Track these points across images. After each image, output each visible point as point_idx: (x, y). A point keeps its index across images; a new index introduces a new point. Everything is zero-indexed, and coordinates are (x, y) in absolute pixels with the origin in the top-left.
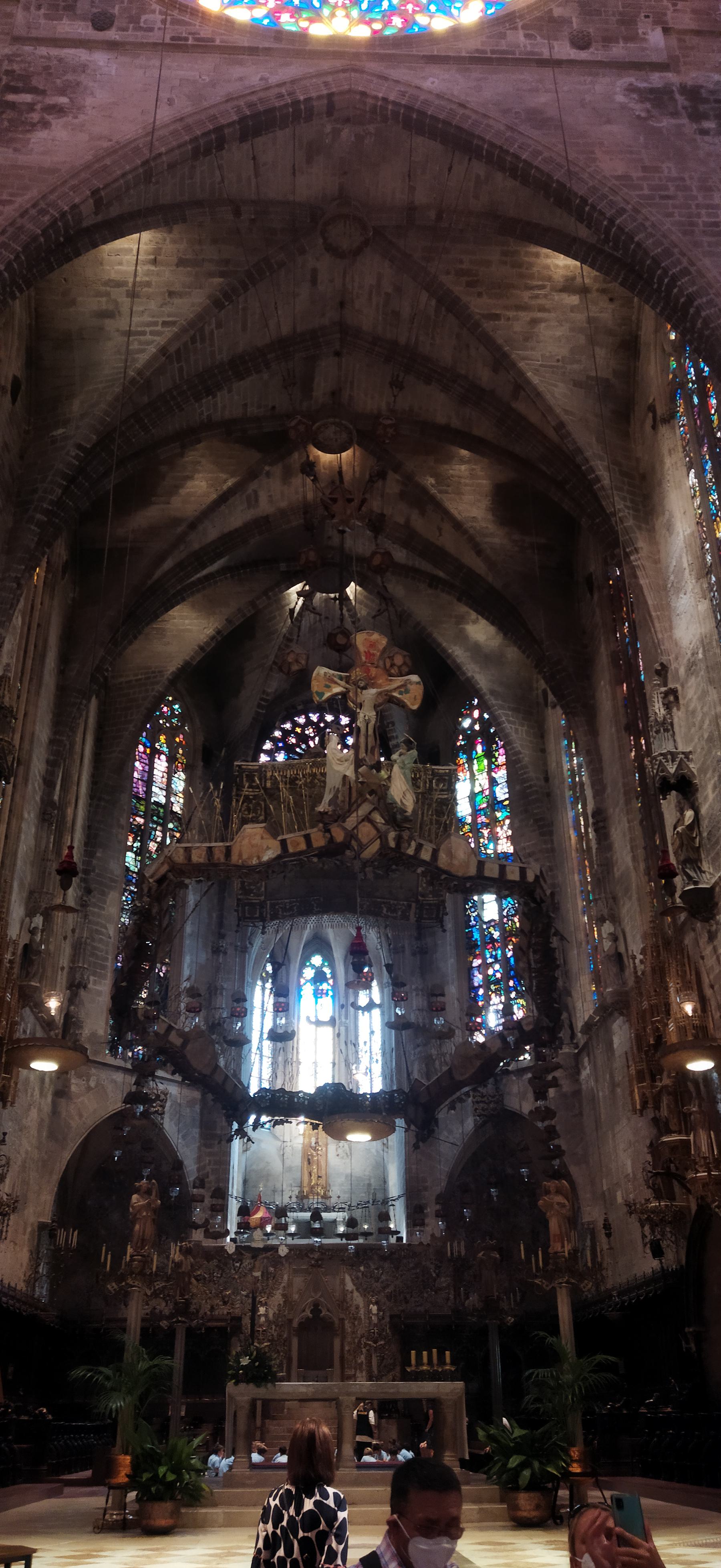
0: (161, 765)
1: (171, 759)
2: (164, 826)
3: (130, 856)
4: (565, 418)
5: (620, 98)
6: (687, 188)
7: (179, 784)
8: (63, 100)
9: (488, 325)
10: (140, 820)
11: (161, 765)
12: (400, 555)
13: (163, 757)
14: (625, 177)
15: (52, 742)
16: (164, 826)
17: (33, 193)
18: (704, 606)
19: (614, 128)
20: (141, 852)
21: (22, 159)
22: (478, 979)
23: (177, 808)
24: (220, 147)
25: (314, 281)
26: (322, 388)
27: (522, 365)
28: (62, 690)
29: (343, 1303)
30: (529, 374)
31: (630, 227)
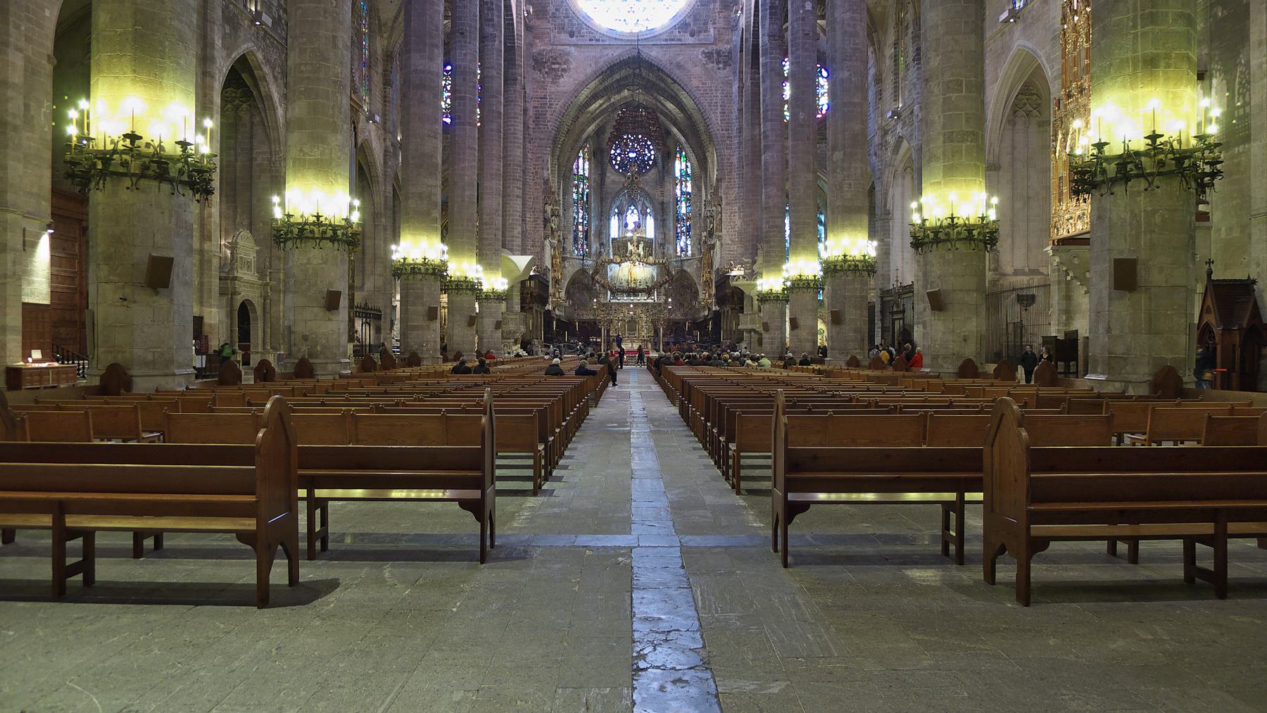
1: (584, 158)
2: (583, 182)
3: (574, 195)
4: (693, 111)
6: (712, 90)
7: (587, 166)
10: (576, 182)
11: (581, 161)
13: (581, 158)
16: (583, 182)
19: (697, 68)
20: (577, 193)
21: (559, 89)
22: (679, 230)
23: (587, 175)
30: (683, 100)
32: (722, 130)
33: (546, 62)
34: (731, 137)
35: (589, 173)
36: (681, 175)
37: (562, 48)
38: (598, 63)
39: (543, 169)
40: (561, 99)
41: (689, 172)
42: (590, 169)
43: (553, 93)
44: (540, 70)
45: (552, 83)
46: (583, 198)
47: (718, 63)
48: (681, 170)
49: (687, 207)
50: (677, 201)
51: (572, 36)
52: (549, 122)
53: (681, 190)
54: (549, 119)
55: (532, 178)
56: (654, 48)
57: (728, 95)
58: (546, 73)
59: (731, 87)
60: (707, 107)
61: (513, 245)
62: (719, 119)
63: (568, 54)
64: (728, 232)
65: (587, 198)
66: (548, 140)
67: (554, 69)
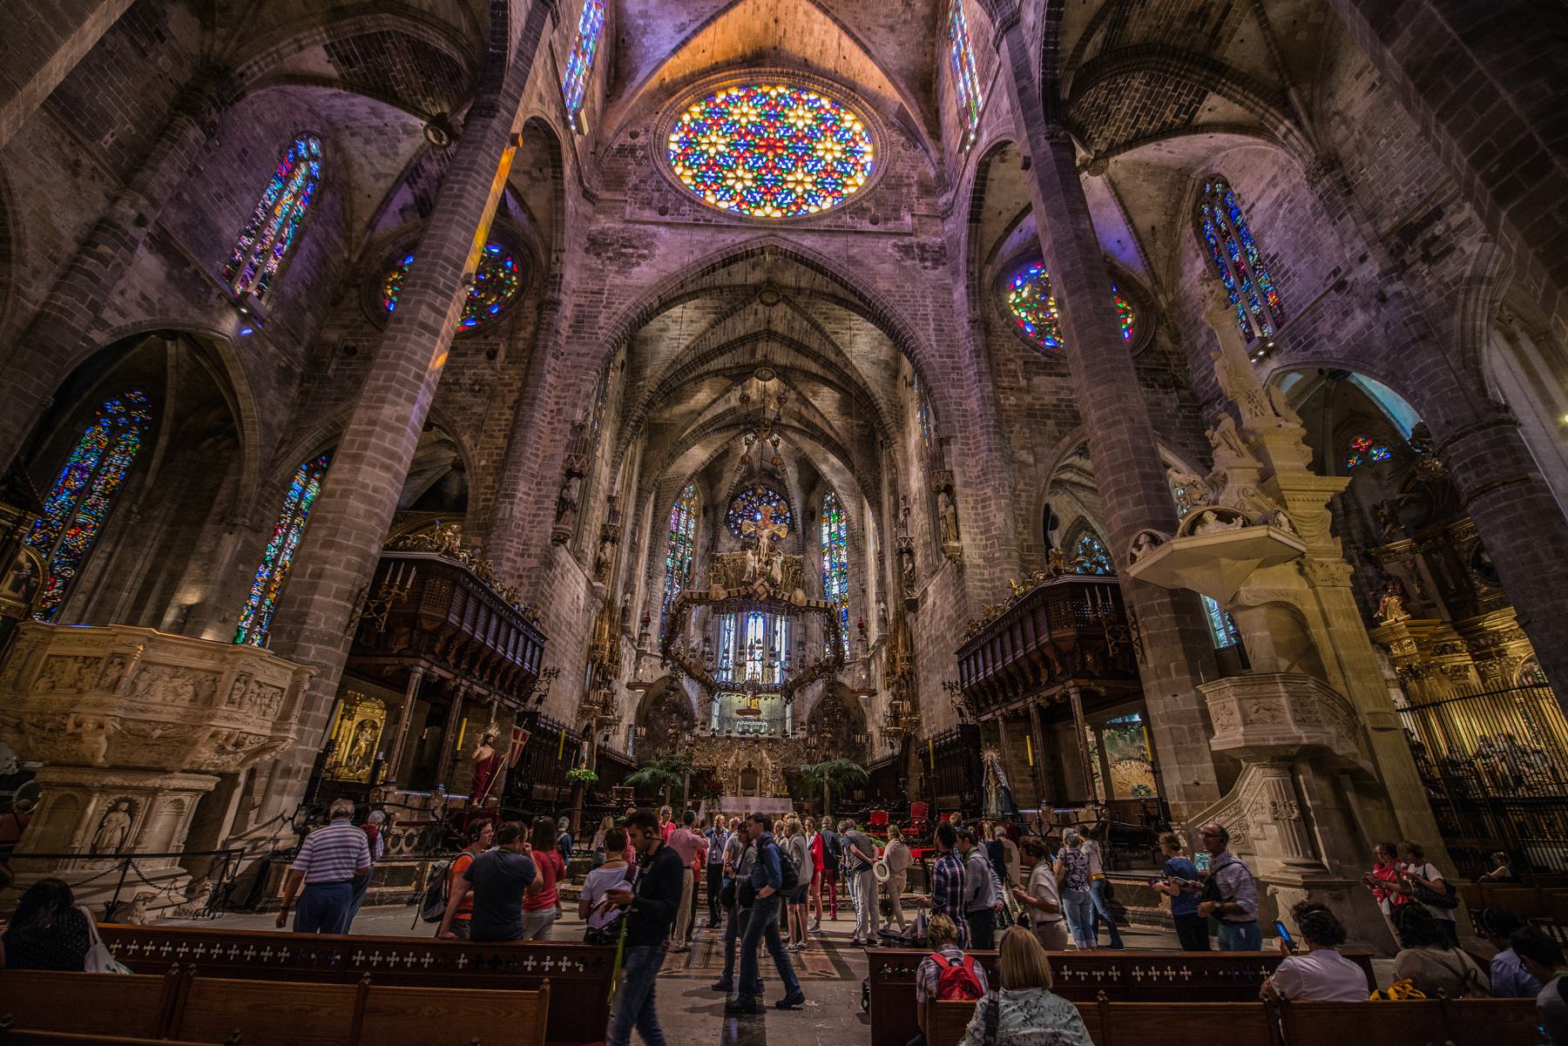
0: (683, 517)
1: (689, 513)
5: (890, 250)
6: (915, 297)
7: (692, 526)
8: (646, 252)
9: (833, 337)
11: (683, 517)
12: (796, 424)
14: (889, 291)
15: (635, 514)
17: (633, 299)
18: (921, 474)
19: (886, 266)
21: (628, 282)
24: (714, 270)
25: (756, 314)
26: (759, 356)
27: (848, 355)
28: (640, 490)
29: (762, 763)
31: (889, 315)
32: (941, 356)
33: (612, 244)
34: (960, 368)
35: (696, 535)
36: (831, 542)
37: (642, 227)
38: (706, 250)
39: (575, 405)
40: (630, 296)
41: (843, 534)
42: (696, 529)
43: (617, 286)
44: (598, 255)
45: (616, 272)
46: (681, 568)
47: (923, 260)
48: (830, 534)
49: (840, 584)
50: (824, 577)
51: (663, 211)
52: (600, 328)
53: (830, 561)
54: (601, 324)
55: (548, 419)
56: (809, 235)
57: (945, 306)
58: (609, 258)
59: (951, 294)
60: (908, 320)
61: (365, 446)
62: (933, 338)
63: (654, 235)
64: (974, 540)
65: (689, 568)
66: (593, 358)
67: (624, 255)
